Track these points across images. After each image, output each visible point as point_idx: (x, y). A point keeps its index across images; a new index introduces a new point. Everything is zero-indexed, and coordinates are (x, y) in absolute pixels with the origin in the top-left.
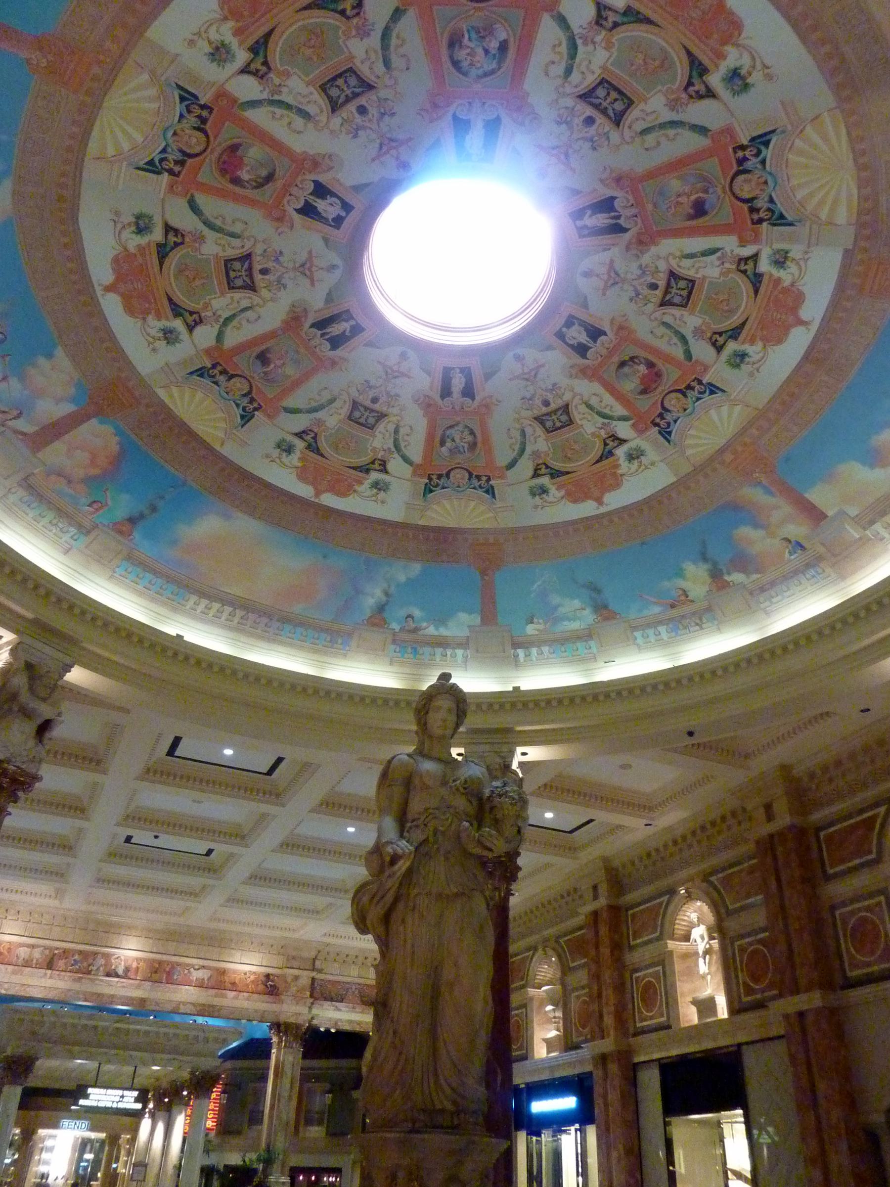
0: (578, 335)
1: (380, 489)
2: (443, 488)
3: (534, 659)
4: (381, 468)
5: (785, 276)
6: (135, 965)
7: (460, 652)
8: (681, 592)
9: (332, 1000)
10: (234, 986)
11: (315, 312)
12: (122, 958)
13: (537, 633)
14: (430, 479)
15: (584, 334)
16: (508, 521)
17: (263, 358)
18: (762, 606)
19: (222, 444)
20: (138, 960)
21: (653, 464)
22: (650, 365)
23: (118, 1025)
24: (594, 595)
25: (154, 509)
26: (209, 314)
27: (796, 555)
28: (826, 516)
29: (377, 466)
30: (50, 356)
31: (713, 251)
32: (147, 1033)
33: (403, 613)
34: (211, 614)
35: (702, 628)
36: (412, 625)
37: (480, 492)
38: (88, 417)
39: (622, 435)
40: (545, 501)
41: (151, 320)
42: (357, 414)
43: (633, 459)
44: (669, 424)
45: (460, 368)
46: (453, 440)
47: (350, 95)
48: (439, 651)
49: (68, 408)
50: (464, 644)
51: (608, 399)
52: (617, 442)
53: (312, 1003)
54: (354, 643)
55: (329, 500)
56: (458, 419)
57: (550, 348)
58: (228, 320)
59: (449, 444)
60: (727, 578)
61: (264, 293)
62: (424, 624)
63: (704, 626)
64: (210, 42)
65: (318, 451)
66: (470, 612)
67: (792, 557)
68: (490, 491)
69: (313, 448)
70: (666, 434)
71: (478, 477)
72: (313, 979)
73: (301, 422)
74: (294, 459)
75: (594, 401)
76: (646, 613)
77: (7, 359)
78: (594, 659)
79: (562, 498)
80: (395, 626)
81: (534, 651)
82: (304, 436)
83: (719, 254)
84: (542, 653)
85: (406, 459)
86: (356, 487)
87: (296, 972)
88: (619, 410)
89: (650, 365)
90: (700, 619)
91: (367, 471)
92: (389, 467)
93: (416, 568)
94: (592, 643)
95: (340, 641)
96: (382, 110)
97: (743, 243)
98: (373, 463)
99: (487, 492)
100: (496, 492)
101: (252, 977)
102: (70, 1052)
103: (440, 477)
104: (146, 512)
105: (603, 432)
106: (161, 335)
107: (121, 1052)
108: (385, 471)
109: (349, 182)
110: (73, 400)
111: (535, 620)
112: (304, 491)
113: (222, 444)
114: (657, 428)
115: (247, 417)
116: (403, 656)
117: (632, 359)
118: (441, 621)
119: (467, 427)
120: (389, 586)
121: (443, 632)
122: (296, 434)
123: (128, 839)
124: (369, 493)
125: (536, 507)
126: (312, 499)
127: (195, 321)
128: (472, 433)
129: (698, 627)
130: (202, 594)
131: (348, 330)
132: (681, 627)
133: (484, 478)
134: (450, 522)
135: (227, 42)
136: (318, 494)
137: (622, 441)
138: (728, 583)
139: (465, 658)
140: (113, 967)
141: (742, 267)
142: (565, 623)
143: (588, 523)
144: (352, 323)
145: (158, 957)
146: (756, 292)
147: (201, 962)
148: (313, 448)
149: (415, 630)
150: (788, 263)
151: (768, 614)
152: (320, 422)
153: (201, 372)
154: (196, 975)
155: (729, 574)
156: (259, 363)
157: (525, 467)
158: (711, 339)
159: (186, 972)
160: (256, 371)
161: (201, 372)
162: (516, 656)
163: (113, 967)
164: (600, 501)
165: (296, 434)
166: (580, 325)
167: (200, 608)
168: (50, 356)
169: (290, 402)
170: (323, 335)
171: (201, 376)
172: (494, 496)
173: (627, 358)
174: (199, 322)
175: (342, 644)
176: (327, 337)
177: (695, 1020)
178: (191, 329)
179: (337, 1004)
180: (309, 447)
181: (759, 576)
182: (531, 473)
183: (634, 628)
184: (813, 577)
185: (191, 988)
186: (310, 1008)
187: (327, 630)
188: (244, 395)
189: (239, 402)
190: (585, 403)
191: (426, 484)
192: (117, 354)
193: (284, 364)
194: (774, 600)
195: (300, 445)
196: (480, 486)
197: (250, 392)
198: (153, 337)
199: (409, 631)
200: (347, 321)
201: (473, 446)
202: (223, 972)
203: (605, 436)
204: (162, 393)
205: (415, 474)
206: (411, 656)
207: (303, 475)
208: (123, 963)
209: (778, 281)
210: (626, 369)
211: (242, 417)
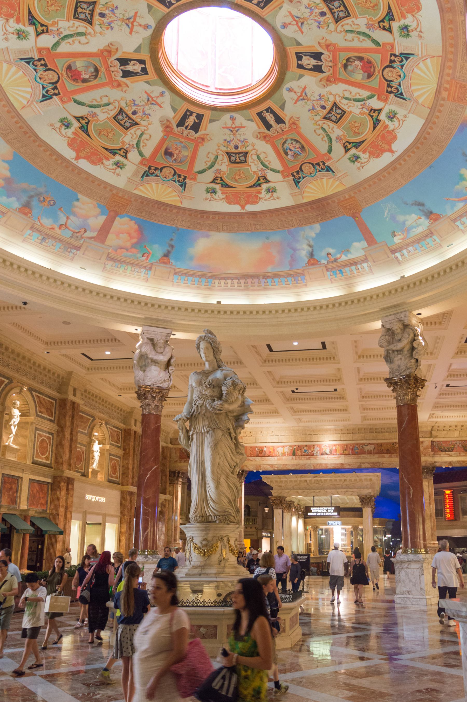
2: (304, 178)
4: (265, 180)
7: (365, 265)
11: (173, 118)
16: (349, 182)
19: (181, 203)
21: (405, 117)
23: (315, 479)
24: (421, 208)
30: (78, 200)
32: (331, 480)
33: (324, 253)
36: (333, 258)
37: (324, 172)
38: (115, 218)
42: (233, 159)
46: (290, 150)
47: (90, 12)
48: (353, 268)
49: (102, 219)
50: (365, 260)
54: (307, 277)
56: (285, 137)
59: (290, 153)
62: (338, 256)
64: (13, 34)
66: (359, 241)
68: (329, 169)
71: (318, 164)
76: (456, 209)
77: (62, 209)
80: (324, 262)
82: (216, 181)
86: (260, 196)
93: (317, 227)
96: (110, 9)
99: (327, 170)
102: (298, 492)
107: (322, 491)
108: (268, 181)
109: (132, 50)
110: (102, 213)
111: (396, 234)
113: (181, 203)
116: (336, 277)
118: (347, 251)
119: (292, 139)
120: (309, 242)
121: (350, 256)
122: (212, 182)
125: (359, 168)
128: (297, 141)
134: (321, 195)
135: (18, 29)
139: (369, 267)
143: (392, 166)
144: (194, 115)
148: (224, 185)
149: (335, 260)
152: (219, 171)
153: (146, 174)
156: (168, 157)
160: (170, 161)
161: (146, 174)
165: (212, 182)
168: (78, 200)
170: (186, 128)
174: (126, 152)
176: (189, 127)
178: (126, 157)
187: (289, 276)
188: (174, 175)
190: (344, 98)
192: (106, 185)
193: (180, 151)
199: (332, 262)
200: (191, 115)
201: (303, 148)
205: (284, 177)
206: (341, 275)
207: (229, 201)
211: (181, 186)
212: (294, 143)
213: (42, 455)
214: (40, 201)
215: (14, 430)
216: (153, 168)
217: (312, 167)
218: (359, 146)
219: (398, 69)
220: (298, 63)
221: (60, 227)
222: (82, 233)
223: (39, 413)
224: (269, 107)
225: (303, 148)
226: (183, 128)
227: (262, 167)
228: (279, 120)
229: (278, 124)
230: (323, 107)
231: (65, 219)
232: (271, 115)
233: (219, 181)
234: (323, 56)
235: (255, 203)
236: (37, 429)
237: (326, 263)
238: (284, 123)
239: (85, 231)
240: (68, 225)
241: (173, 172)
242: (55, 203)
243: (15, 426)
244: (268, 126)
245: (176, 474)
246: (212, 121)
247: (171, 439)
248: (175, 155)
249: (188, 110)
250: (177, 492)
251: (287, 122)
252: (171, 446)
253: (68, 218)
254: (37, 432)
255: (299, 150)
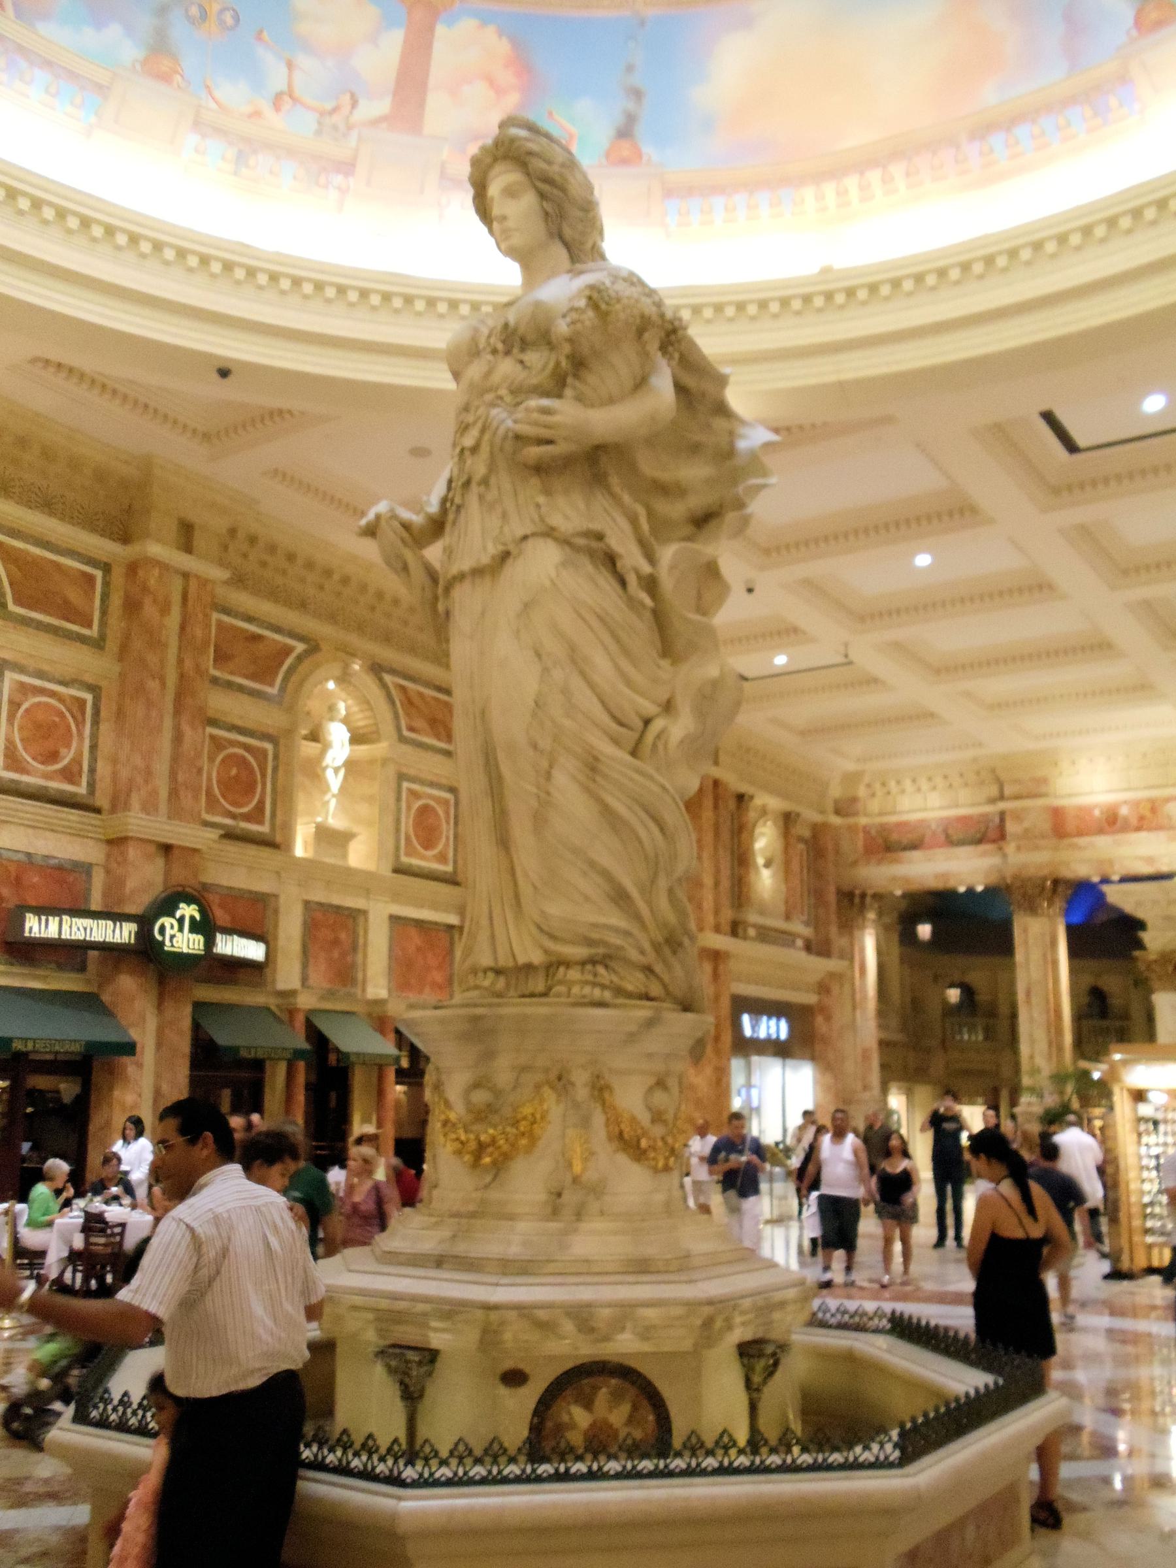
25: (637, 94)
38: (431, 29)
49: (393, 42)
77: (265, 35)
104: (631, 106)
130: (819, 177)
213: (426, 848)
214: (192, 20)
215: (334, 781)
221: (277, 102)
222: (346, 109)
223: (406, 733)
231: (284, 70)
236: (401, 777)
239: (354, 103)
240: (297, 93)
242: (237, 18)
243: (336, 770)
245: (857, 900)
247: (836, 802)
250: (862, 950)
252: (836, 820)
253: (290, 65)
254: (405, 785)
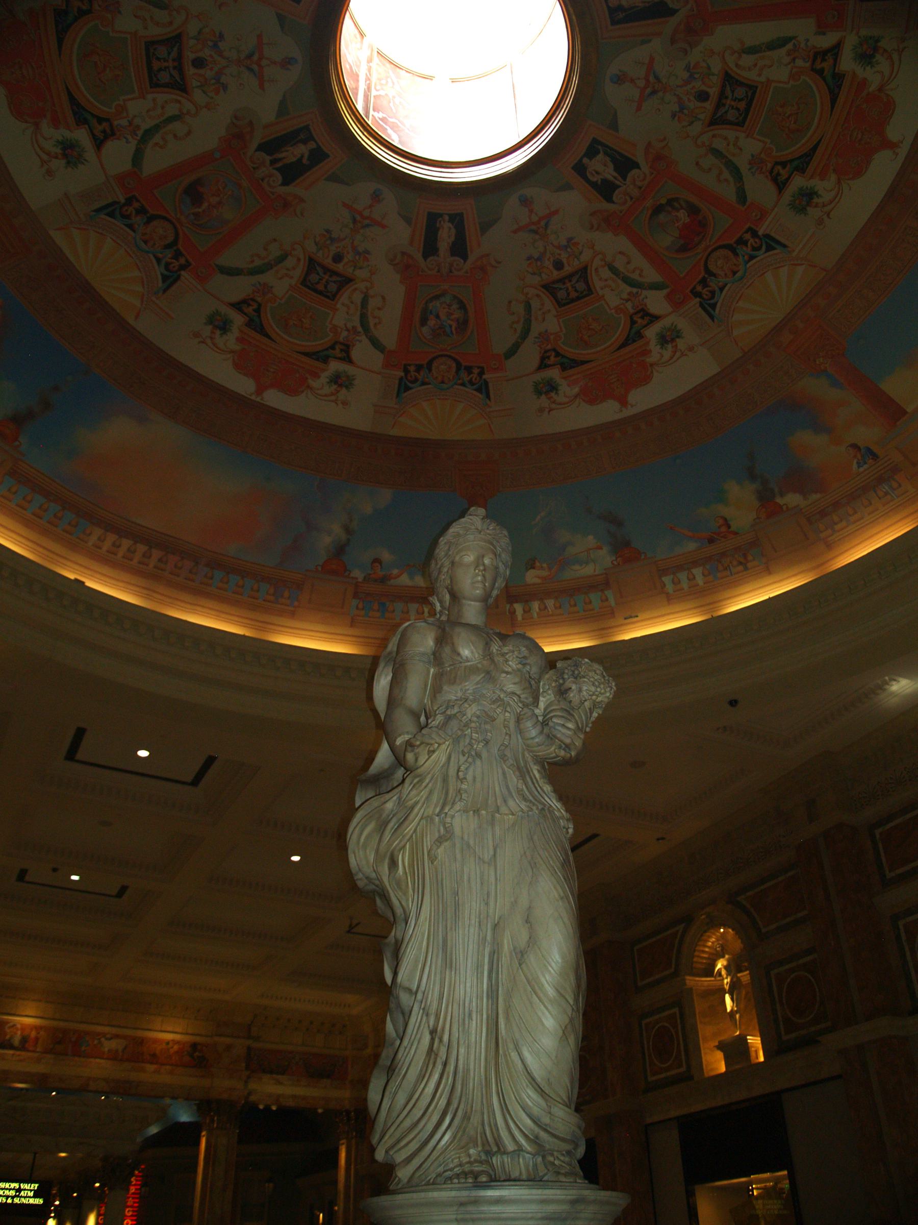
0: (602, 168)
1: (341, 386)
2: (423, 384)
3: (535, 615)
5: (872, 76)
6: (33, 1034)
8: (721, 521)
9: (271, 1072)
10: (154, 1058)
12: (19, 1026)
13: (538, 581)
14: (406, 371)
15: (611, 166)
17: (194, 193)
18: (822, 535)
19: (137, 316)
20: (38, 1028)
22: (693, 210)
26: (124, 122)
27: (866, 466)
28: (905, 413)
29: (337, 352)
31: (781, 43)
34: (120, 554)
35: (746, 569)
39: (654, 309)
40: (554, 402)
41: (46, 128)
43: (667, 342)
44: (713, 293)
45: (449, 215)
46: (438, 316)
51: (639, 260)
52: (647, 319)
53: (249, 1077)
55: (274, 399)
57: (567, 187)
58: (149, 134)
59: (432, 322)
60: (779, 500)
61: (198, 96)
62: (395, 572)
63: (749, 565)
65: (262, 331)
67: (861, 469)
68: (484, 388)
69: (256, 325)
70: (709, 307)
71: (469, 370)
72: (249, 1048)
73: (240, 288)
74: (230, 340)
75: (619, 264)
78: (612, 614)
79: (576, 396)
80: (358, 574)
81: (536, 605)
83: (790, 46)
84: (546, 608)
85: (376, 343)
87: (228, 1040)
88: (652, 275)
89: (693, 210)
90: (745, 556)
91: (326, 360)
92: (355, 354)
94: (609, 594)
95: (286, 594)
97: (822, 28)
98: (333, 347)
99: (479, 390)
100: (491, 388)
101: (176, 1047)
103: (419, 368)
105: (629, 305)
106: (58, 150)
108: (348, 359)
112: (244, 385)
113: (137, 316)
114: (698, 299)
115: (170, 279)
117: (670, 202)
119: (455, 297)
123: (22, 875)
124: (327, 390)
125: (541, 410)
126: (253, 397)
127: (104, 131)
128: (463, 306)
129: (741, 568)
131: (306, 156)
132: (720, 568)
133: (476, 371)
136: (260, 390)
137: (655, 318)
138: (781, 507)
140: (8, 1037)
141: (818, 66)
142: (577, 567)
144: (312, 145)
145: (62, 1024)
146: (833, 101)
147: (115, 1031)
148: (256, 325)
149: (383, 580)
150: (878, 57)
151: (829, 546)
153: (111, 209)
154: (109, 1045)
155: (782, 495)
157: (530, 354)
158: (771, 172)
159: (96, 1042)
161: (111, 209)
162: (513, 613)
163: (8, 1037)
164: (624, 402)
166: (606, 154)
167: (107, 545)
169: (227, 259)
170: (273, 162)
171: (111, 215)
172: (488, 396)
173: (663, 201)
174: (111, 134)
175: (289, 598)
176: (279, 165)
177: (722, 1068)
178: (99, 144)
179: (279, 1077)
180: (250, 324)
181: (818, 496)
182: (536, 362)
183: (664, 572)
184: (886, 494)
185: (102, 1061)
186: (246, 1082)
188: (167, 247)
189: (160, 255)
191: (401, 379)
194: (837, 527)
195: (238, 320)
196: (471, 383)
197: (175, 242)
198: (48, 154)
200: (305, 142)
201: (463, 324)
202: (142, 1041)
203: (632, 311)
204: (58, 237)
207: (241, 364)
208: (19, 1033)
209: (864, 83)
210: (662, 217)
212: (455, 306)
216: (136, 205)
217: (454, 370)
218: (571, 367)
219: (741, 259)
220: (581, 160)
224: (461, 215)
225: (463, 324)
226: (268, 158)
227: (357, 323)
228: (460, 249)
229: (452, 255)
230: (559, 265)
232: (453, 231)
233: (250, 310)
234: (635, 172)
235: (292, 392)
237: (360, 580)
238: (465, 257)
241: (170, 239)
244: (430, 249)
246: (334, 178)
248: (205, 205)
249: (307, 128)
251: (472, 258)
255: (454, 325)
